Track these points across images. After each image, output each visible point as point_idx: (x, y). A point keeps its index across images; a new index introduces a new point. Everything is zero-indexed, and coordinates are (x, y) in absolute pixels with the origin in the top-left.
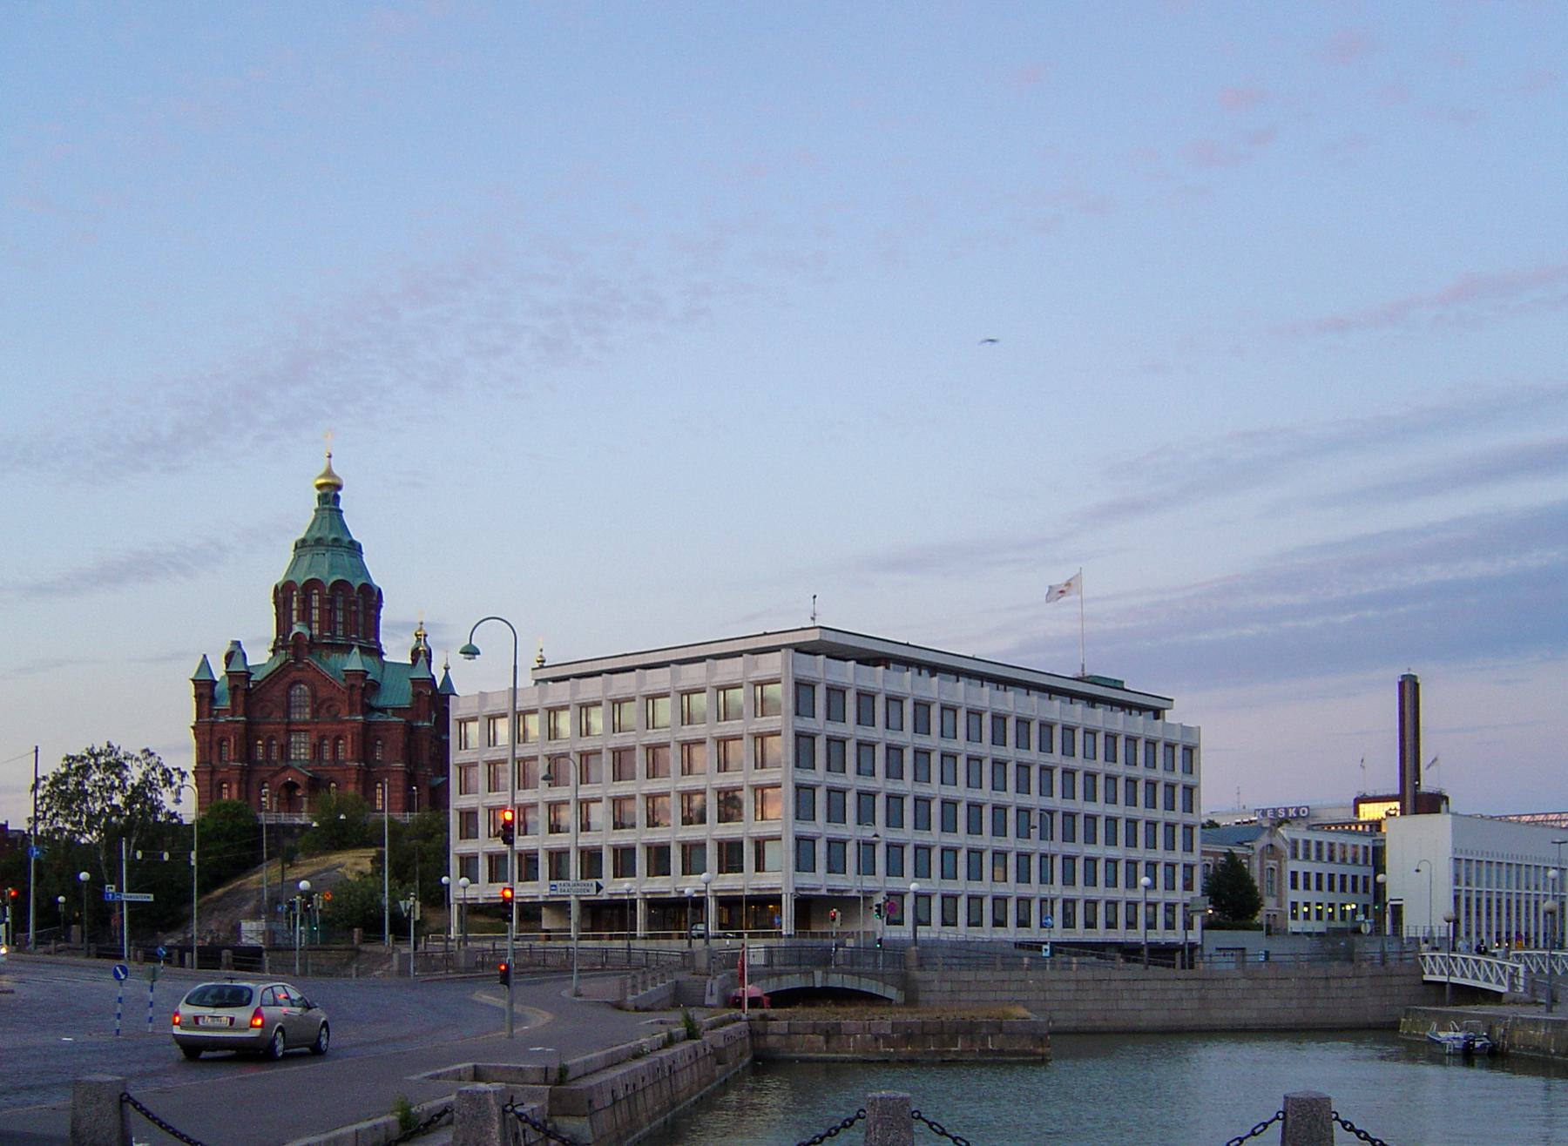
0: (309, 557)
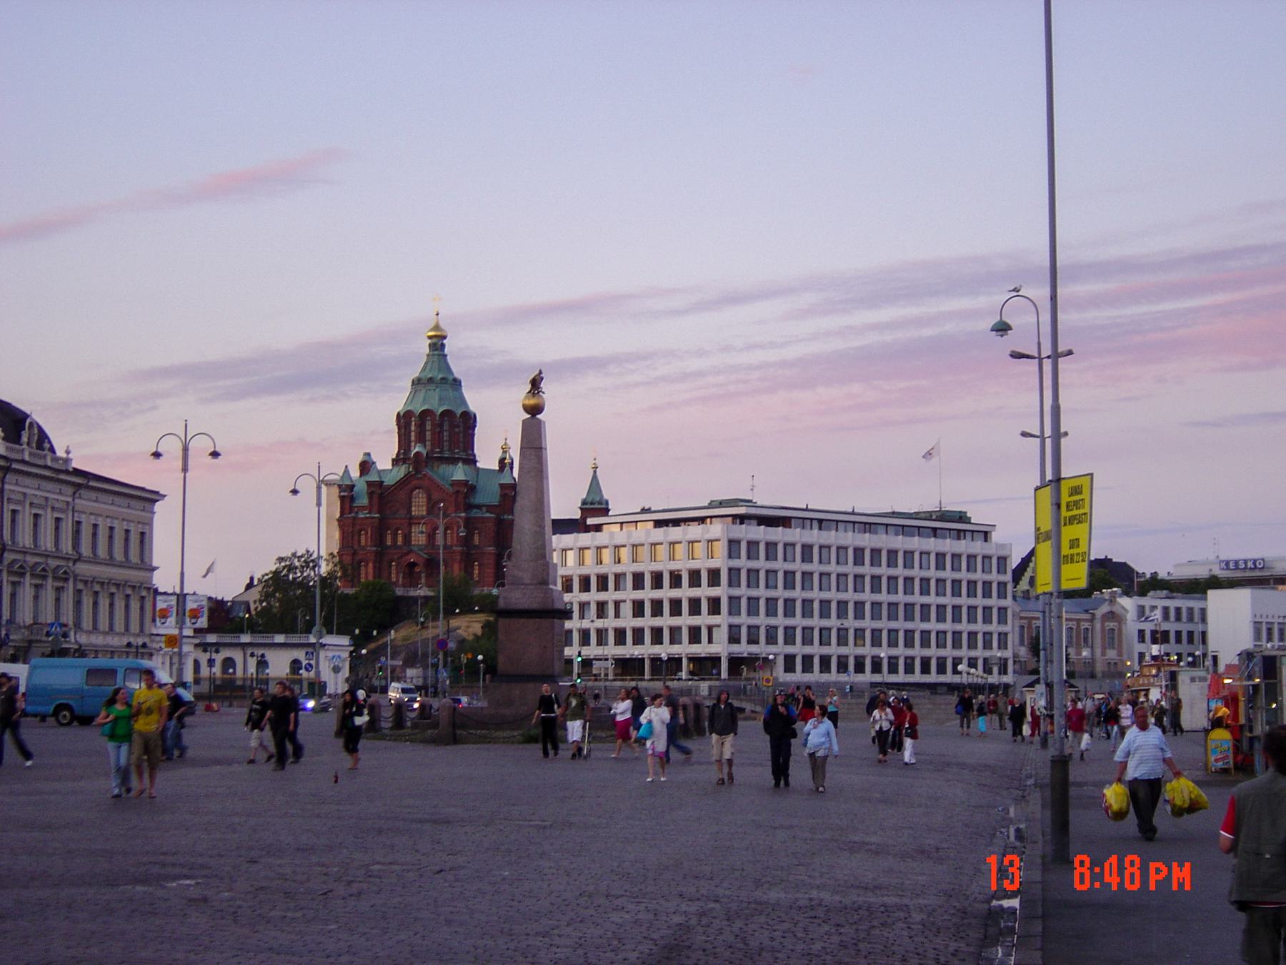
0: (424, 391)
